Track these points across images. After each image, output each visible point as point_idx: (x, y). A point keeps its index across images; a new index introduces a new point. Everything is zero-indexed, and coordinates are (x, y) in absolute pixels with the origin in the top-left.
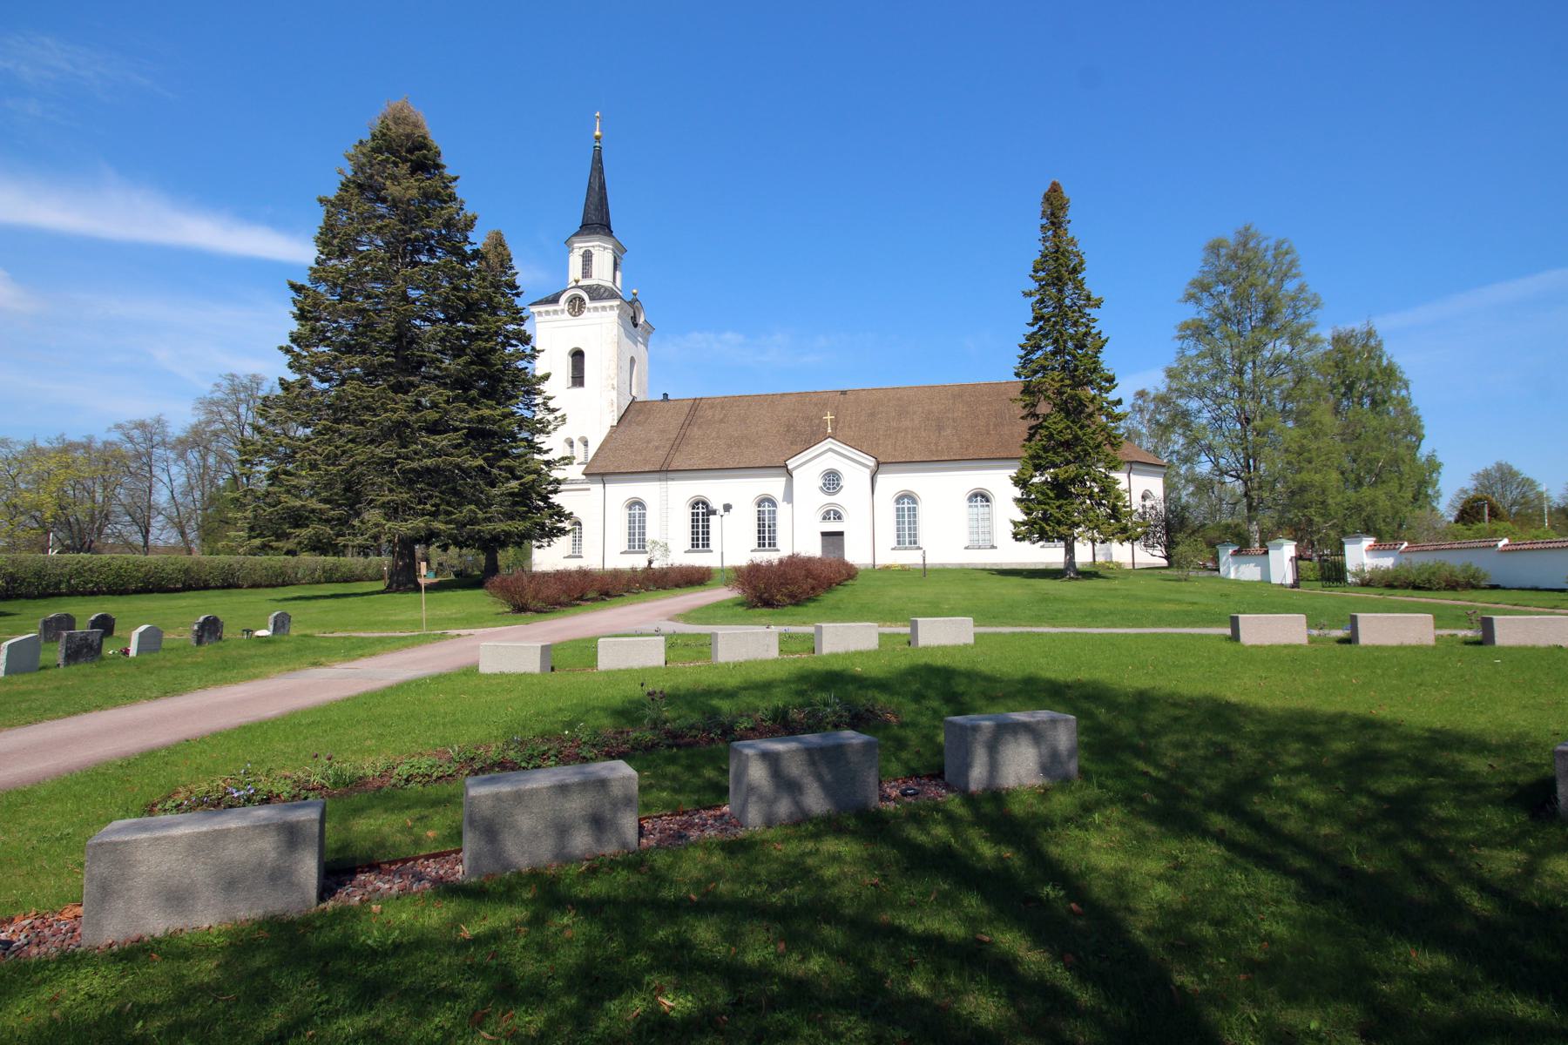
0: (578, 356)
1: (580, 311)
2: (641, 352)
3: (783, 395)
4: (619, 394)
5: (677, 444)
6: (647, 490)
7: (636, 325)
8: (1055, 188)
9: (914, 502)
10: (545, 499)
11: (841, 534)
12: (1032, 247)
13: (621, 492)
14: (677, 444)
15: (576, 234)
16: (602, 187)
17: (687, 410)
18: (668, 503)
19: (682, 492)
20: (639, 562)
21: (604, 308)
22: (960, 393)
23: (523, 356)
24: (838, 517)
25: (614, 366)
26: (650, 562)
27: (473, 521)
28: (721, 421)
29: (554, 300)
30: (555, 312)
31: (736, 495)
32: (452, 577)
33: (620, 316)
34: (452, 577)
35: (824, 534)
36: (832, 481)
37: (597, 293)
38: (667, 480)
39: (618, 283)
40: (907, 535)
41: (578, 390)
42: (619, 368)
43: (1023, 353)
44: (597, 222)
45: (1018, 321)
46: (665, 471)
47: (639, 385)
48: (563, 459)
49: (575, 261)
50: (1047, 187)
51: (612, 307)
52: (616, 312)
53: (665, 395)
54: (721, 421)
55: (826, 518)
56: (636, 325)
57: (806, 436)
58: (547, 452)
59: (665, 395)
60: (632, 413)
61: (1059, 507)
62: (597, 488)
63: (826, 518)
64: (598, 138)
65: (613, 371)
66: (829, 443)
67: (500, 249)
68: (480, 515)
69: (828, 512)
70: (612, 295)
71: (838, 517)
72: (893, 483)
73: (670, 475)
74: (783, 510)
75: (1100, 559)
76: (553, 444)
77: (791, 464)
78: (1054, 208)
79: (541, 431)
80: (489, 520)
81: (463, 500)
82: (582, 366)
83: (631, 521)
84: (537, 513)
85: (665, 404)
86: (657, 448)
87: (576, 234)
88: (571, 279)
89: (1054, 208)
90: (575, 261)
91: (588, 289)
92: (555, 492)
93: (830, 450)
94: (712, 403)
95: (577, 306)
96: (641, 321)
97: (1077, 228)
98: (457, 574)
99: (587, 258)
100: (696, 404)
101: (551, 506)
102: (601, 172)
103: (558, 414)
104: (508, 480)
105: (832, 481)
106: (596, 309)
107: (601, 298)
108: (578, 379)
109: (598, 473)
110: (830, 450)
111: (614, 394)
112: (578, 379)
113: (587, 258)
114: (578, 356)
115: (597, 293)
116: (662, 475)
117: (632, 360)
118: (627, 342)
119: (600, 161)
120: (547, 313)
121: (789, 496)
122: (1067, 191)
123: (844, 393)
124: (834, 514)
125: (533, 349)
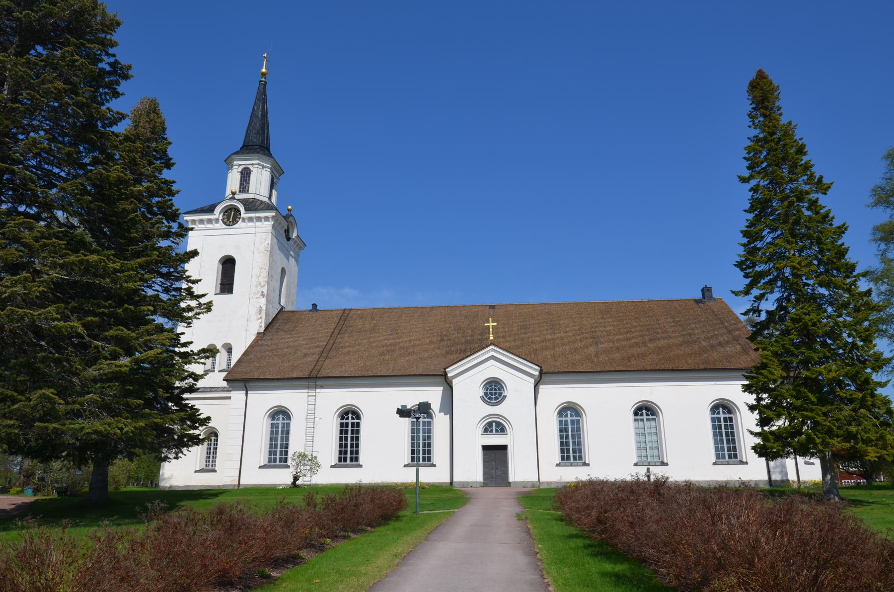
0: (228, 264)
1: (235, 221)
2: (292, 266)
3: (432, 308)
4: (267, 301)
5: (327, 351)
6: (293, 399)
7: (288, 239)
8: (761, 75)
9: (578, 414)
10: (178, 400)
11: (504, 448)
12: (743, 132)
13: (264, 400)
14: (327, 351)
15: (237, 153)
16: (265, 114)
17: (336, 320)
18: (315, 413)
19: (332, 400)
20: (282, 477)
21: (259, 219)
22: (607, 309)
23: (167, 235)
24: (501, 429)
25: (265, 273)
26: (296, 478)
27: (50, 415)
28: (372, 330)
29: (210, 210)
30: (210, 221)
31: (381, 407)
32: (55, 495)
33: (274, 227)
34: (55, 495)
35: (485, 448)
36: (494, 391)
37: (252, 205)
38: (316, 387)
39: (274, 200)
40: (571, 448)
41: (226, 297)
42: (270, 276)
43: (745, 240)
44: (257, 143)
45: (731, 208)
46: (313, 379)
47: (288, 295)
48: (203, 351)
49: (233, 180)
50: (752, 75)
51: (267, 219)
52: (269, 224)
53: (315, 305)
54: (372, 330)
55: (488, 429)
56: (288, 239)
57: (468, 345)
58: (185, 345)
59: (315, 305)
60: (278, 323)
61: (825, 414)
62: (238, 396)
63: (488, 429)
64: (263, 74)
65: (263, 279)
66: (490, 351)
67: (152, 116)
68: (62, 408)
69: (490, 424)
70: (268, 207)
71: (501, 429)
72: (557, 394)
73: (319, 382)
74: (440, 422)
75: (776, 477)
76: (196, 334)
77: (451, 372)
78: (762, 94)
79: (183, 319)
80: (78, 414)
81: (38, 379)
82: (232, 274)
83: (274, 431)
84: (161, 409)
85: (313, 314)
86: (305, 355)
87: (237, 153)
88: (228, 193)
89: (762, 94)
90: (233, 180)
91: (245, 202)
92: (191, 389)
93: (493, 358)
94: (362, 314)
95: (231, 216)
96: (294, 235)
97: (788, 110)
98: (60, 492)
99: (246, 175)
100: (345, 315)
101: (183, 407)
102: (265, 102)
103: (203, 301)
104: (115, 356)
105: (494, 391)
106: (251, 219)
107: (256, 210)
108: (226, 285)
109: (242, 378)
110: (493, 358)
111: (263, 302)
112: (226, 285)
113: (246, 175)
114: (228, 264)
115: (252, 205)
116: (311, 383)
117: (283, 271)
118: (279, 256)
119: (264, 93)
120: (201, 222)
121: (448, 406)
122: (775, 77)
123: (492, 307)
124: (495, 426)
125: (181, 226)
